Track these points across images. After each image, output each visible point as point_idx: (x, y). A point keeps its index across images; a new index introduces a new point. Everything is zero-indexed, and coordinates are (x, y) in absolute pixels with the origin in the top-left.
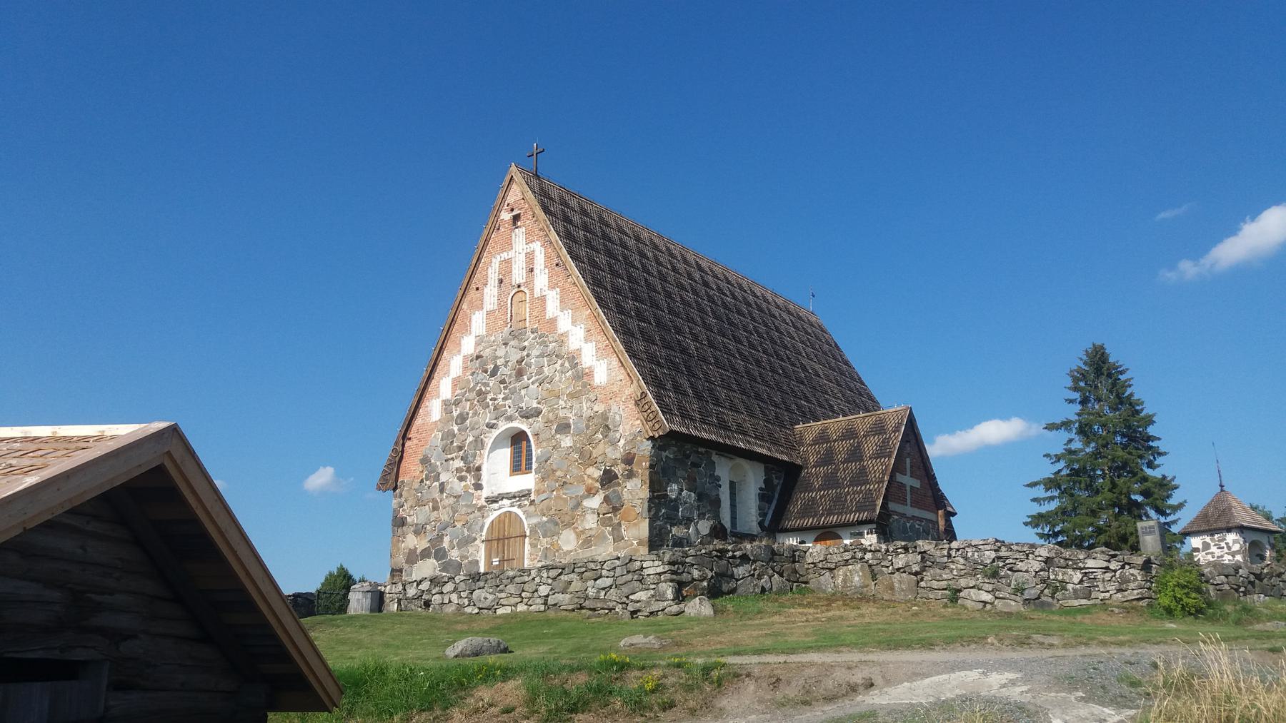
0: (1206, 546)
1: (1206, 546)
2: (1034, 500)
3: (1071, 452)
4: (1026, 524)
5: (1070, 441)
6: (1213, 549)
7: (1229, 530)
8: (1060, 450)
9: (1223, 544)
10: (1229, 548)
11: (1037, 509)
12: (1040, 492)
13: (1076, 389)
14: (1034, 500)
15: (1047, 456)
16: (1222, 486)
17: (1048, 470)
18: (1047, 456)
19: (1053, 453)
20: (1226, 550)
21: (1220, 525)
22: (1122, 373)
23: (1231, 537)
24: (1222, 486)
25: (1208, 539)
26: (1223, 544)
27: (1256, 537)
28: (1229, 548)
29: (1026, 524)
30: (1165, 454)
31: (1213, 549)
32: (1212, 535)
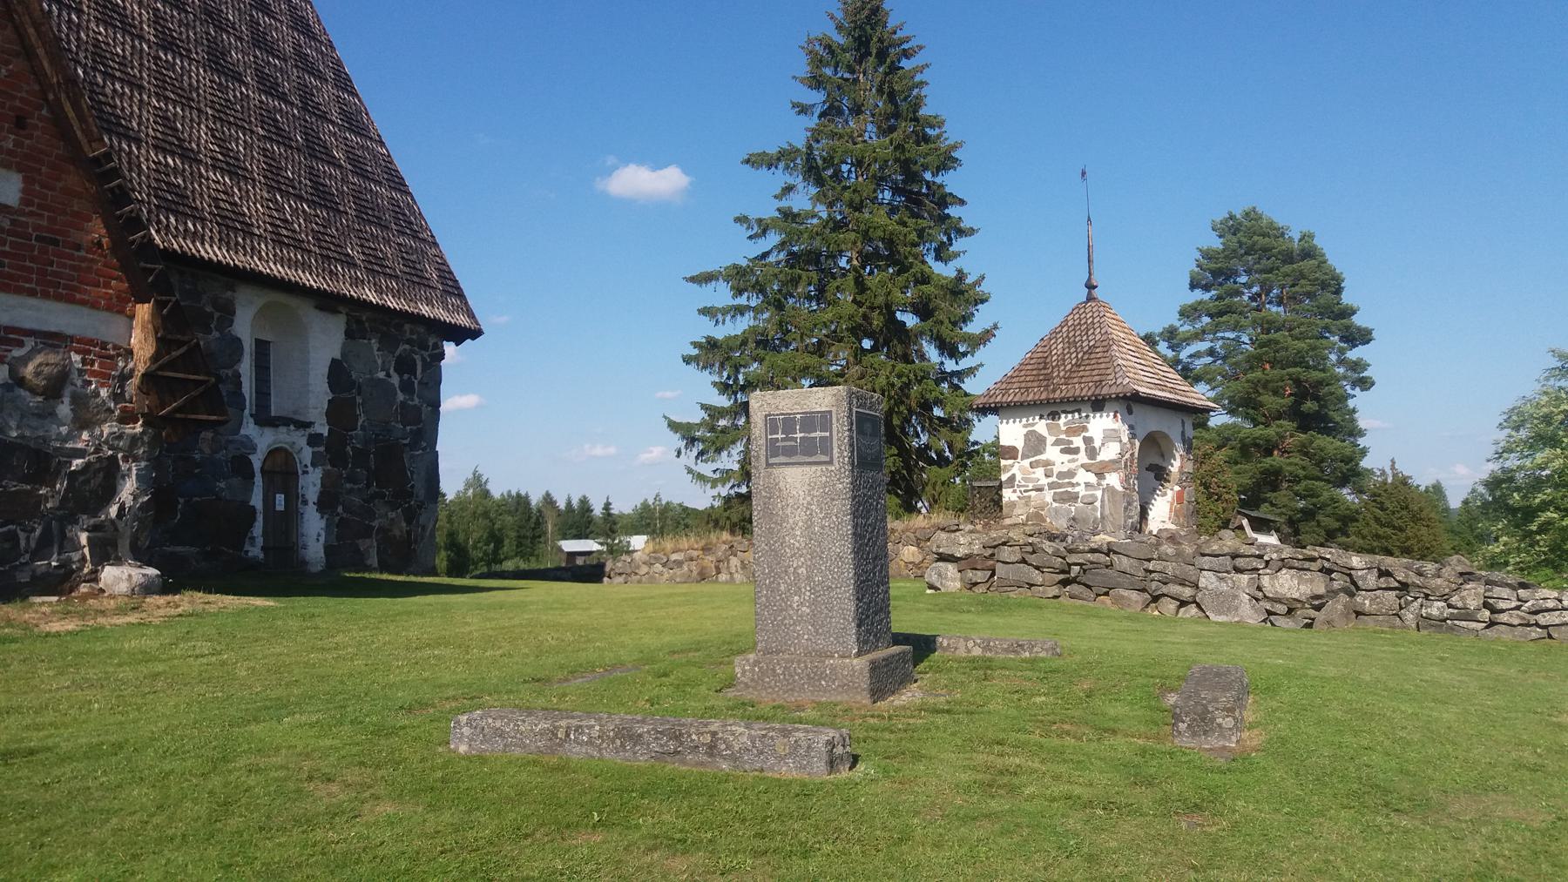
0: (1035, 444)
1: (1035, 444)
2: (705, 311)
3: (788, 215)
4: (687, 360)
5: (788, 189)
6: (1052, 453)
7: (1098, 405)
8: (768, 209)
9: (1078, 442)
10: (1092, 453)
11: (707, 329)
12: (721, 294)
13: (816, 82)
14: (705, 311)
15: (742, 220)
16: (1090, 287)
17: (742, 250)
18: (742, 220)
19: (753, 215)
20: (1082, 458)
21: (1077, 390)
22: (907, 54)
23: (1101, 424)
24: (1090, 287)
25: (1041, 426)
26: (1078, 442)
27: (1154, 422)
28: (1092, 453)
29: (687, 360)
30: (971, 232)
31: (1052, 453)
32: (1054, 415)
